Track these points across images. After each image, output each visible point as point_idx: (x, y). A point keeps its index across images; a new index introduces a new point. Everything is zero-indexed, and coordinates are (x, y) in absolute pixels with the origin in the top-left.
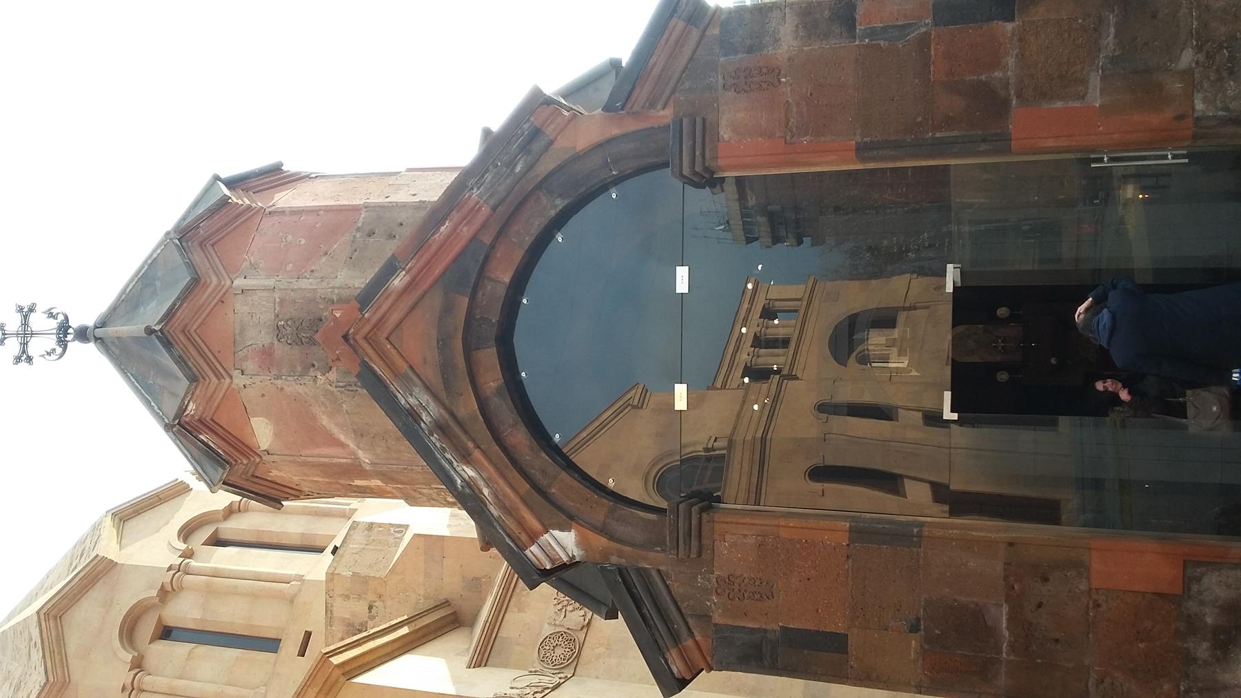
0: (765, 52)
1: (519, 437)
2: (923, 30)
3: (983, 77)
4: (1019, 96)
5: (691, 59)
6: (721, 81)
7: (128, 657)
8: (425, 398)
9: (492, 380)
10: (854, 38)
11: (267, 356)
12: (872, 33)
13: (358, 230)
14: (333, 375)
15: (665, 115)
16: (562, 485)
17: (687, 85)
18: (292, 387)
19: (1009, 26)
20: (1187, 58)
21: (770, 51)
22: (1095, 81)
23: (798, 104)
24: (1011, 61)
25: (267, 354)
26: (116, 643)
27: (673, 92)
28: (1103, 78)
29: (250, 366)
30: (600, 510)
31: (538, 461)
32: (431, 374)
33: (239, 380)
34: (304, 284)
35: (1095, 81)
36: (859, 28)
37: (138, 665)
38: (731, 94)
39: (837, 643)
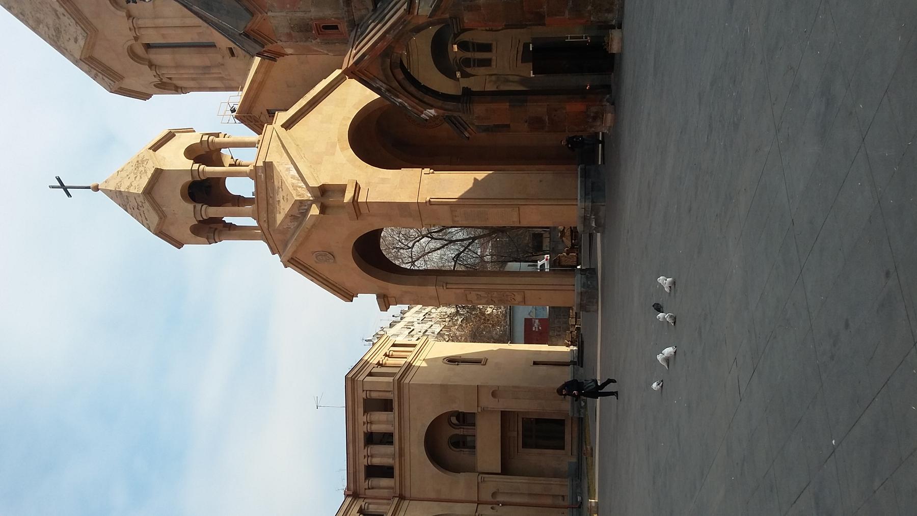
1: (412, 89)
7: (124, 14)
8: (381, 83)
9: (401, 76)
11: (289, 35)
14: (318, 40)
15: (447, 16)
16: (427, 99)
18: (302, 44)
20: (589, 8)
22: (567, 12)
25: (289, 35)
26: (112, 8)
29: (283, 39)
30: (440, 103)
31: (419, 94)
32: (383, 78)
33: (280, 43)
34: (299, 14)
35: (567, 12)
37: (129, 16)
39: (508, 126)
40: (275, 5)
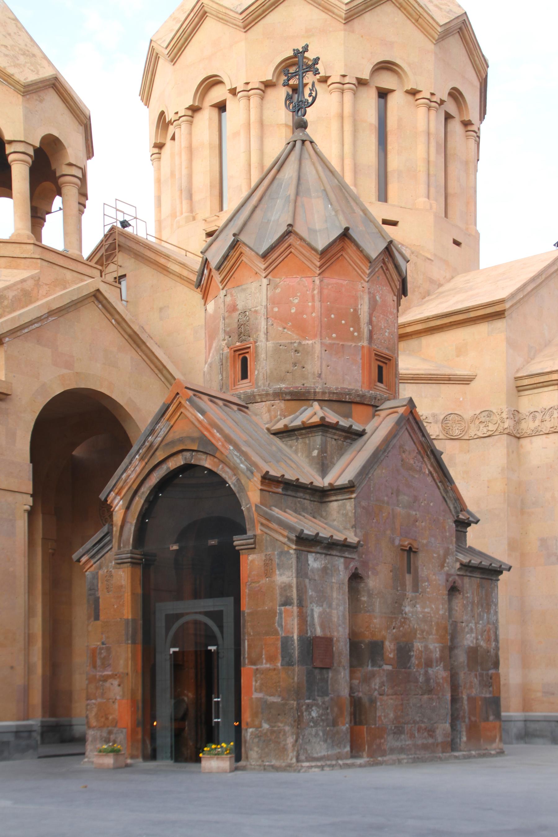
0: (277, 570)
2: (280, 633)
3: (263, 656)
4: (257, 669)
5: (277, 540)
6: (268, 553)
10: (280, 606)
12: (281, 613)
13: (300, 343)
17: (268, 539)
19: (279, 664)
21: (277, 572)
23: (259, 586)
24: (268, 666)
27: (266, 533)
28: (261, 698)
36: (283, 608)
38: (264, 558)
40: (278, 291)
